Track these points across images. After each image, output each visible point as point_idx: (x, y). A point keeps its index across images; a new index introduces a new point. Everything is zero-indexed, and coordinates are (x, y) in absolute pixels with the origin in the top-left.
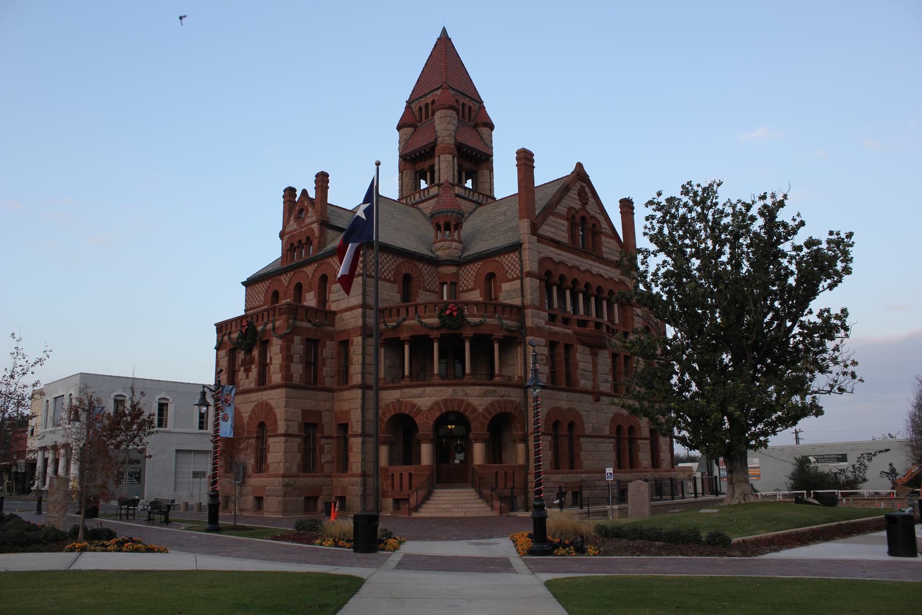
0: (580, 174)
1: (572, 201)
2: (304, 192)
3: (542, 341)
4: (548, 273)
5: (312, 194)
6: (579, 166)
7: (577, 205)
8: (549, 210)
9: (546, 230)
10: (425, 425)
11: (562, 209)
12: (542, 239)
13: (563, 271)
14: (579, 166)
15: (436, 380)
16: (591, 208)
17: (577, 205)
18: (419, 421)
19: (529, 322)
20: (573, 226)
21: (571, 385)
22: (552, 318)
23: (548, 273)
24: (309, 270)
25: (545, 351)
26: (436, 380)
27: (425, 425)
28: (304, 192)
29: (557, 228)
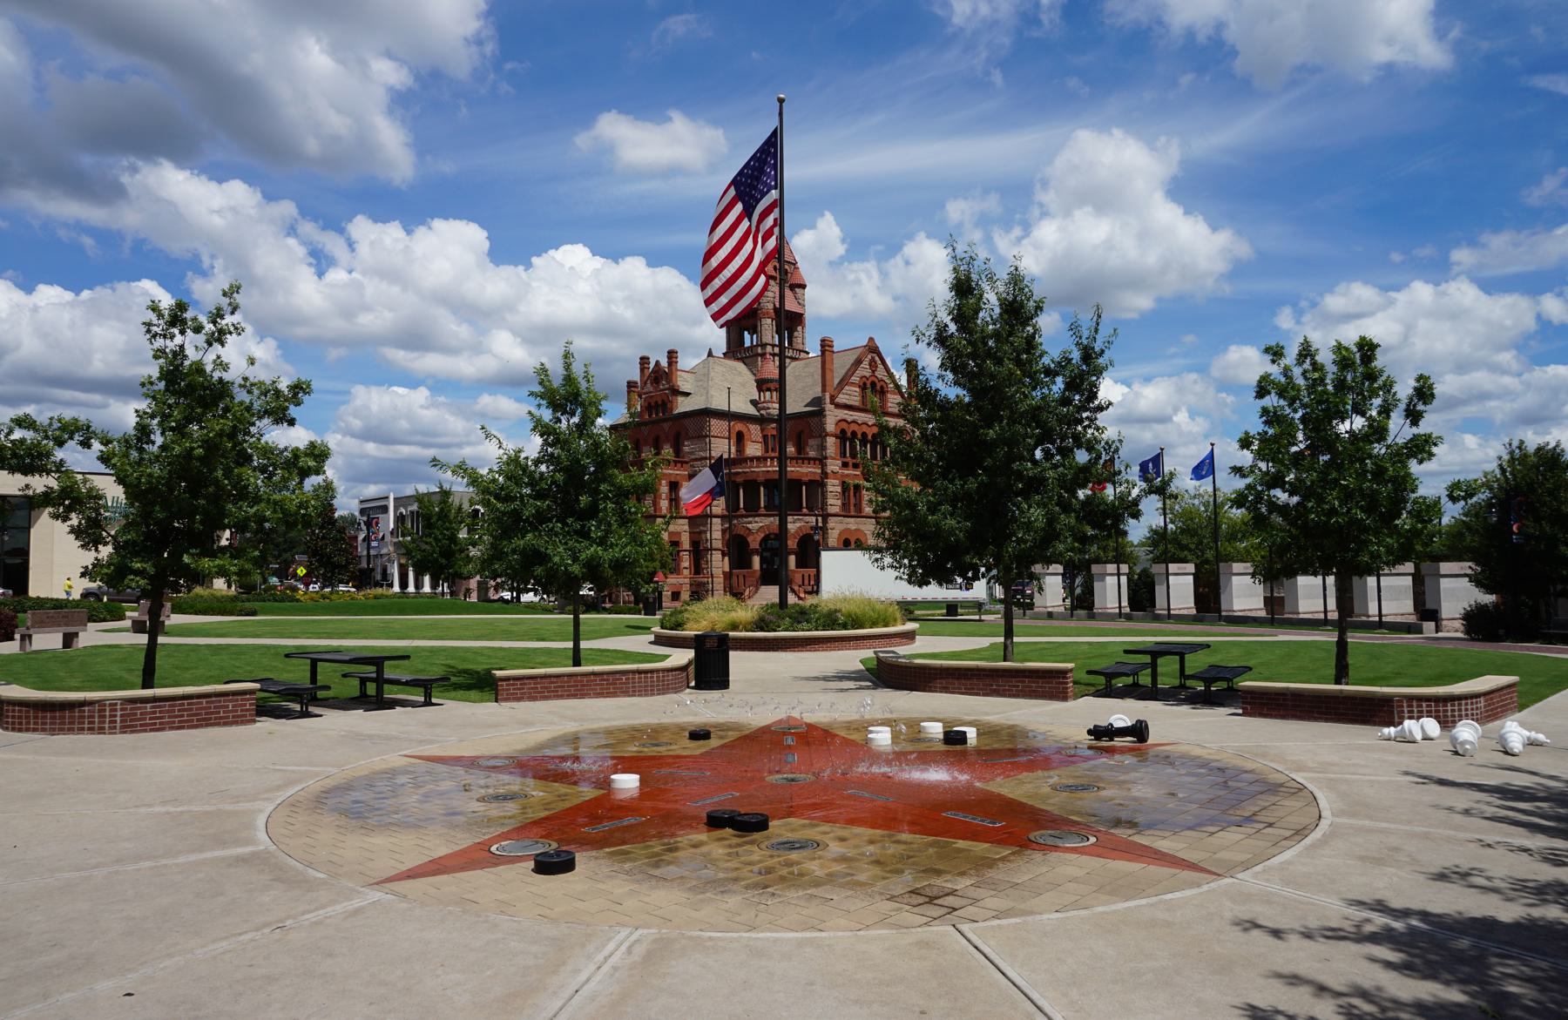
0: (872, 348)
1: (864, 370)
2: (657, 363)
3: (836, 482)
4: (843, 431)
5: (664, 363)
6: (871, 339)
7: (867, 373)
8: (844, 381)
9: (841, 399)
10: (754, 543)
11: (855, 379)
12: (838, 406)
13: (854, 427)
14: (871, 339)
15: (762, 511)
16: (881, 373)
17: (867, 373)
18: (750, 539)
19: (829, 469)
20: (863, 387)
21: (859, 514)
22: (845, 465)
23: (843, 431)
24: (666, 426)
25: (839, 489)
26: (762, 511)
27: (754, 543)
28: (657, 363)
29: (851, 395)
